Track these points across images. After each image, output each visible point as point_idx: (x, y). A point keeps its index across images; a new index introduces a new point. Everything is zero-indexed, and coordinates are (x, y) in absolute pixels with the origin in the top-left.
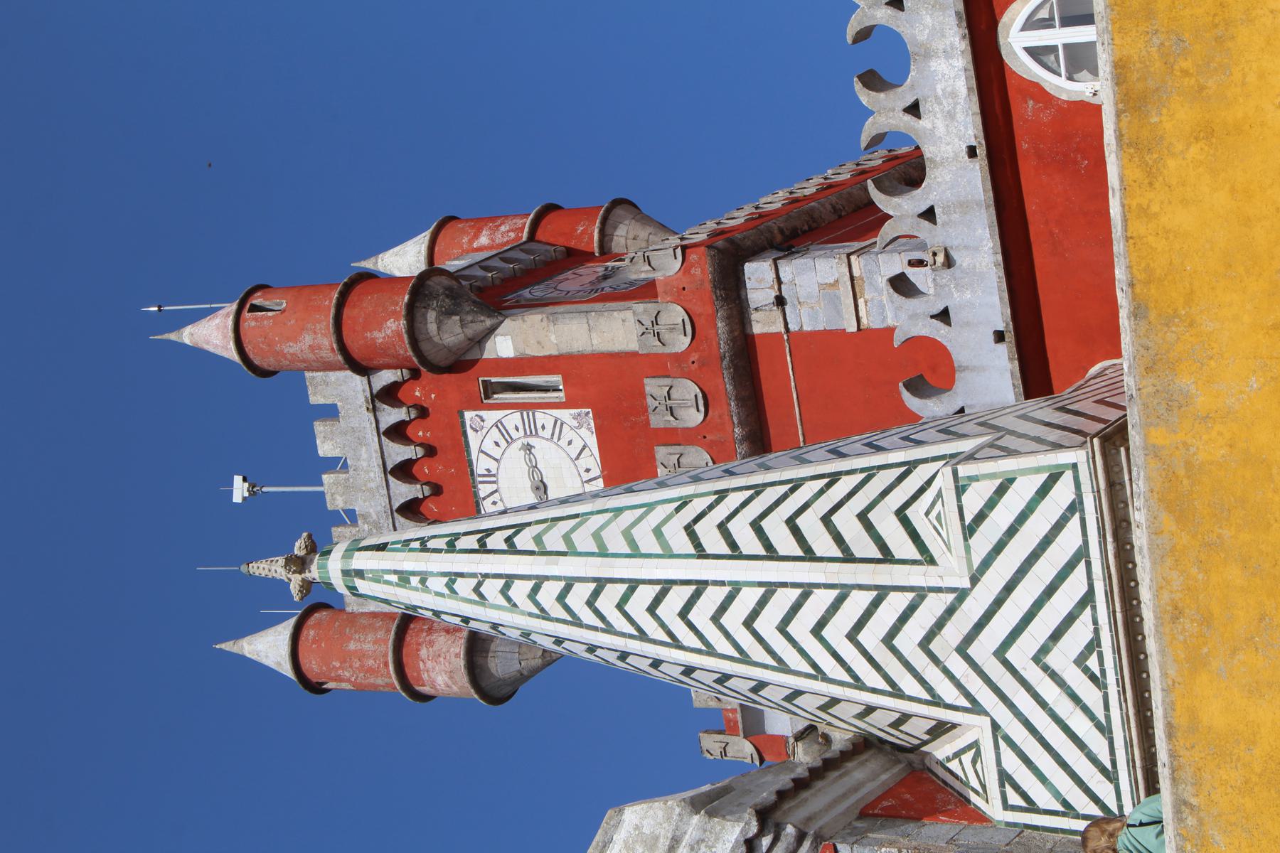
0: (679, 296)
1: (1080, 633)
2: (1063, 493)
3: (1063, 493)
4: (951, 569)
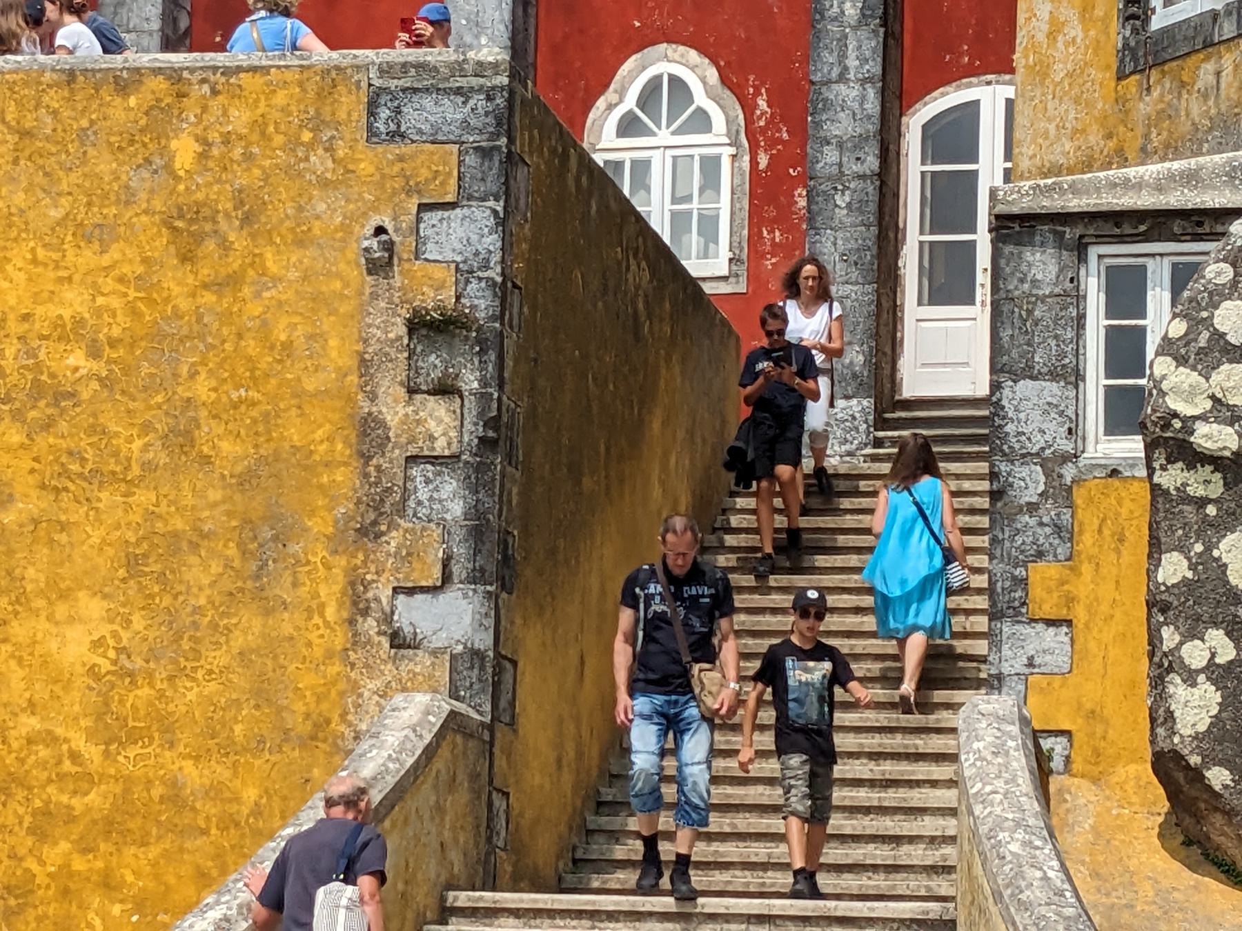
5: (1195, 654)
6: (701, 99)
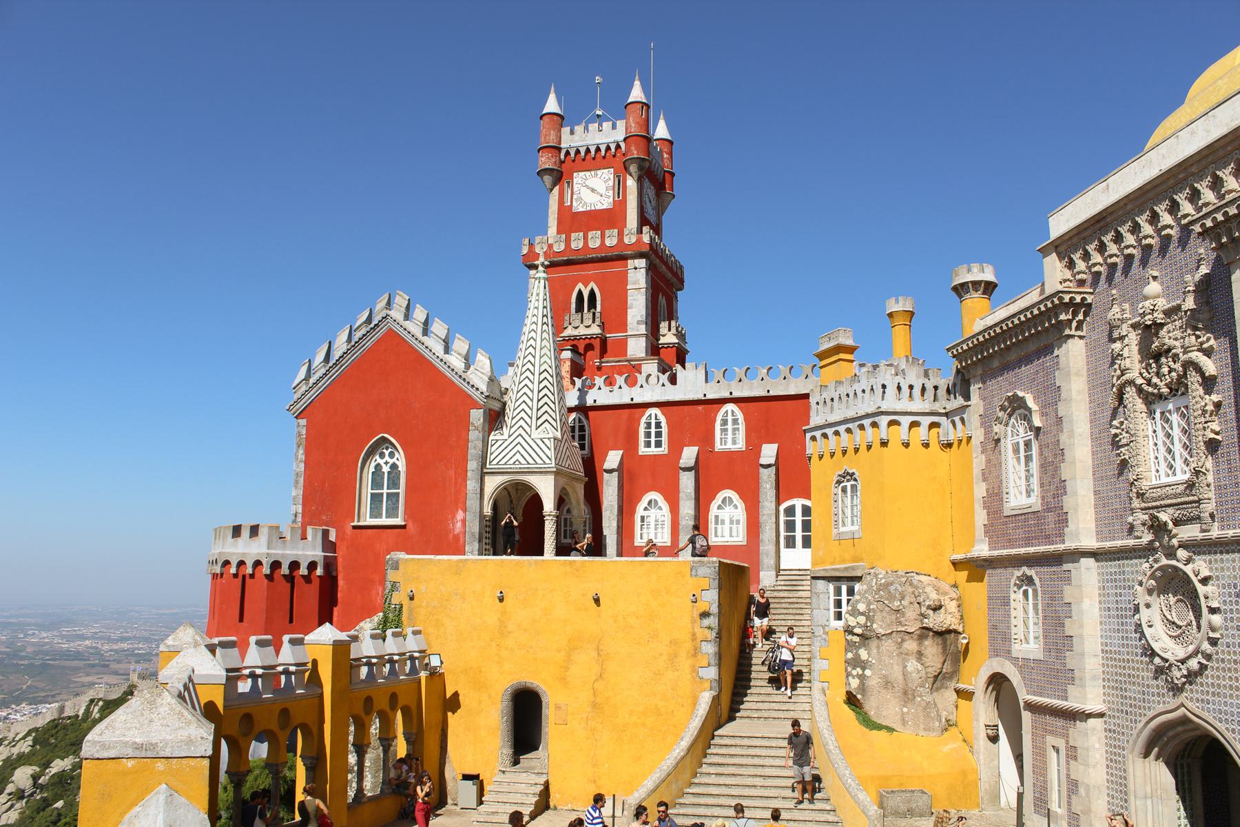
0: (639, 241)
1: (523, 461)
2: (547, 461)
3: (547, 461)
4: (535, 434)
5: (854, 672)
6: (735, 502)
